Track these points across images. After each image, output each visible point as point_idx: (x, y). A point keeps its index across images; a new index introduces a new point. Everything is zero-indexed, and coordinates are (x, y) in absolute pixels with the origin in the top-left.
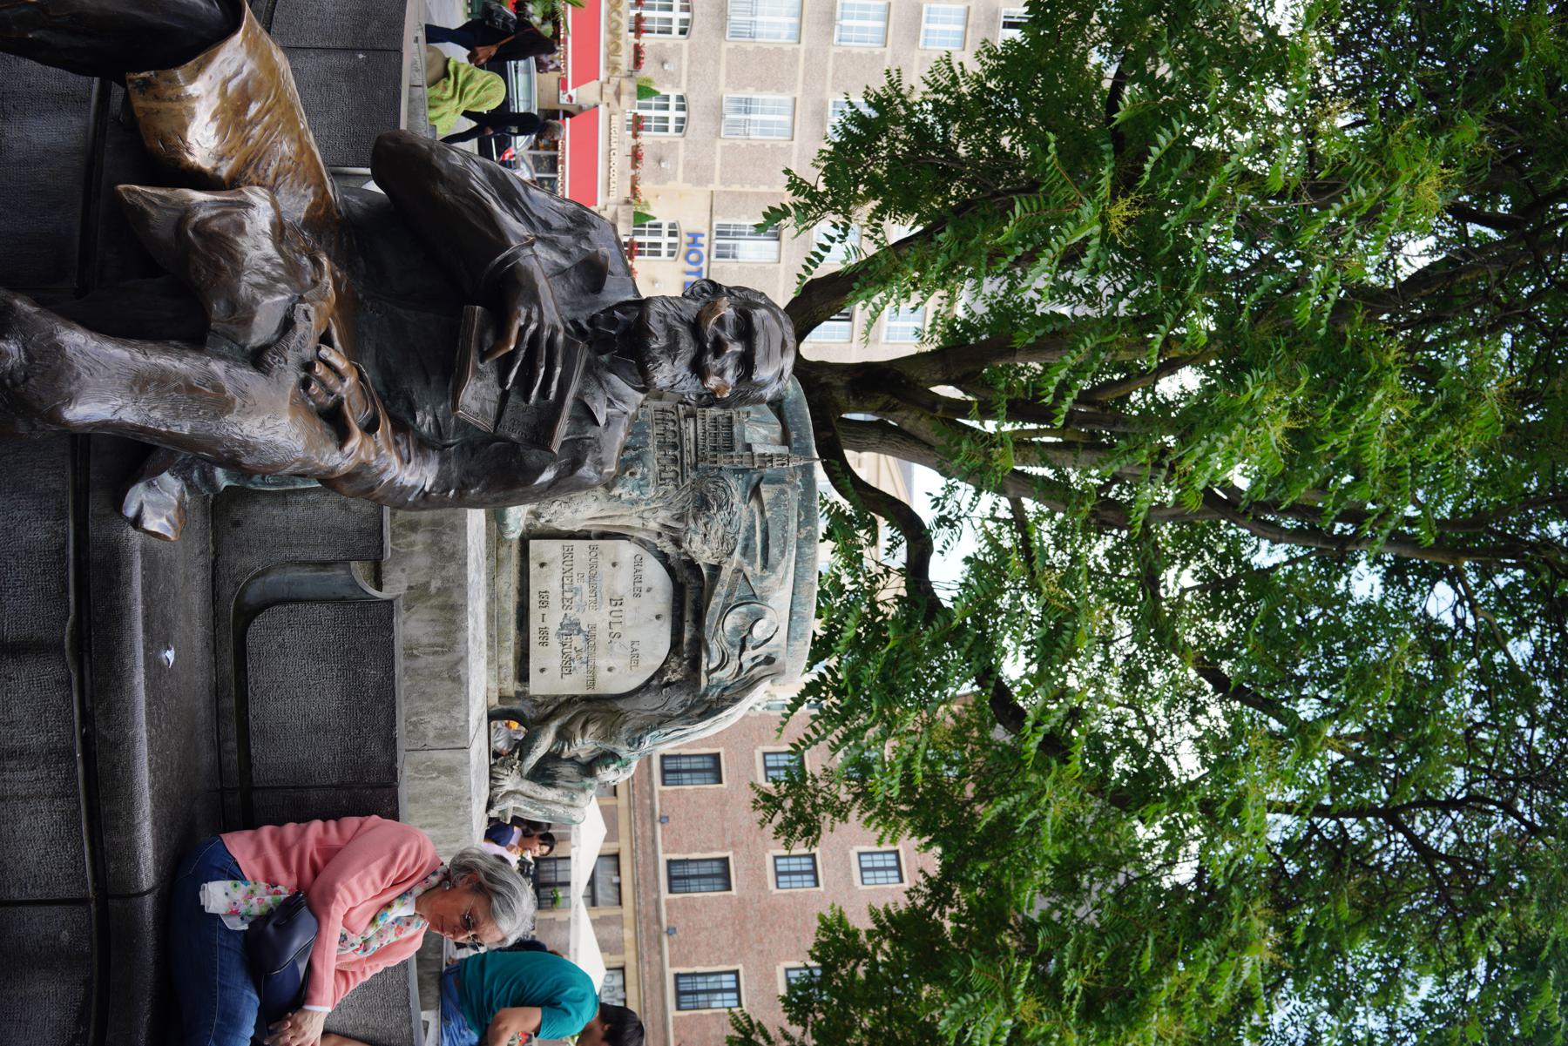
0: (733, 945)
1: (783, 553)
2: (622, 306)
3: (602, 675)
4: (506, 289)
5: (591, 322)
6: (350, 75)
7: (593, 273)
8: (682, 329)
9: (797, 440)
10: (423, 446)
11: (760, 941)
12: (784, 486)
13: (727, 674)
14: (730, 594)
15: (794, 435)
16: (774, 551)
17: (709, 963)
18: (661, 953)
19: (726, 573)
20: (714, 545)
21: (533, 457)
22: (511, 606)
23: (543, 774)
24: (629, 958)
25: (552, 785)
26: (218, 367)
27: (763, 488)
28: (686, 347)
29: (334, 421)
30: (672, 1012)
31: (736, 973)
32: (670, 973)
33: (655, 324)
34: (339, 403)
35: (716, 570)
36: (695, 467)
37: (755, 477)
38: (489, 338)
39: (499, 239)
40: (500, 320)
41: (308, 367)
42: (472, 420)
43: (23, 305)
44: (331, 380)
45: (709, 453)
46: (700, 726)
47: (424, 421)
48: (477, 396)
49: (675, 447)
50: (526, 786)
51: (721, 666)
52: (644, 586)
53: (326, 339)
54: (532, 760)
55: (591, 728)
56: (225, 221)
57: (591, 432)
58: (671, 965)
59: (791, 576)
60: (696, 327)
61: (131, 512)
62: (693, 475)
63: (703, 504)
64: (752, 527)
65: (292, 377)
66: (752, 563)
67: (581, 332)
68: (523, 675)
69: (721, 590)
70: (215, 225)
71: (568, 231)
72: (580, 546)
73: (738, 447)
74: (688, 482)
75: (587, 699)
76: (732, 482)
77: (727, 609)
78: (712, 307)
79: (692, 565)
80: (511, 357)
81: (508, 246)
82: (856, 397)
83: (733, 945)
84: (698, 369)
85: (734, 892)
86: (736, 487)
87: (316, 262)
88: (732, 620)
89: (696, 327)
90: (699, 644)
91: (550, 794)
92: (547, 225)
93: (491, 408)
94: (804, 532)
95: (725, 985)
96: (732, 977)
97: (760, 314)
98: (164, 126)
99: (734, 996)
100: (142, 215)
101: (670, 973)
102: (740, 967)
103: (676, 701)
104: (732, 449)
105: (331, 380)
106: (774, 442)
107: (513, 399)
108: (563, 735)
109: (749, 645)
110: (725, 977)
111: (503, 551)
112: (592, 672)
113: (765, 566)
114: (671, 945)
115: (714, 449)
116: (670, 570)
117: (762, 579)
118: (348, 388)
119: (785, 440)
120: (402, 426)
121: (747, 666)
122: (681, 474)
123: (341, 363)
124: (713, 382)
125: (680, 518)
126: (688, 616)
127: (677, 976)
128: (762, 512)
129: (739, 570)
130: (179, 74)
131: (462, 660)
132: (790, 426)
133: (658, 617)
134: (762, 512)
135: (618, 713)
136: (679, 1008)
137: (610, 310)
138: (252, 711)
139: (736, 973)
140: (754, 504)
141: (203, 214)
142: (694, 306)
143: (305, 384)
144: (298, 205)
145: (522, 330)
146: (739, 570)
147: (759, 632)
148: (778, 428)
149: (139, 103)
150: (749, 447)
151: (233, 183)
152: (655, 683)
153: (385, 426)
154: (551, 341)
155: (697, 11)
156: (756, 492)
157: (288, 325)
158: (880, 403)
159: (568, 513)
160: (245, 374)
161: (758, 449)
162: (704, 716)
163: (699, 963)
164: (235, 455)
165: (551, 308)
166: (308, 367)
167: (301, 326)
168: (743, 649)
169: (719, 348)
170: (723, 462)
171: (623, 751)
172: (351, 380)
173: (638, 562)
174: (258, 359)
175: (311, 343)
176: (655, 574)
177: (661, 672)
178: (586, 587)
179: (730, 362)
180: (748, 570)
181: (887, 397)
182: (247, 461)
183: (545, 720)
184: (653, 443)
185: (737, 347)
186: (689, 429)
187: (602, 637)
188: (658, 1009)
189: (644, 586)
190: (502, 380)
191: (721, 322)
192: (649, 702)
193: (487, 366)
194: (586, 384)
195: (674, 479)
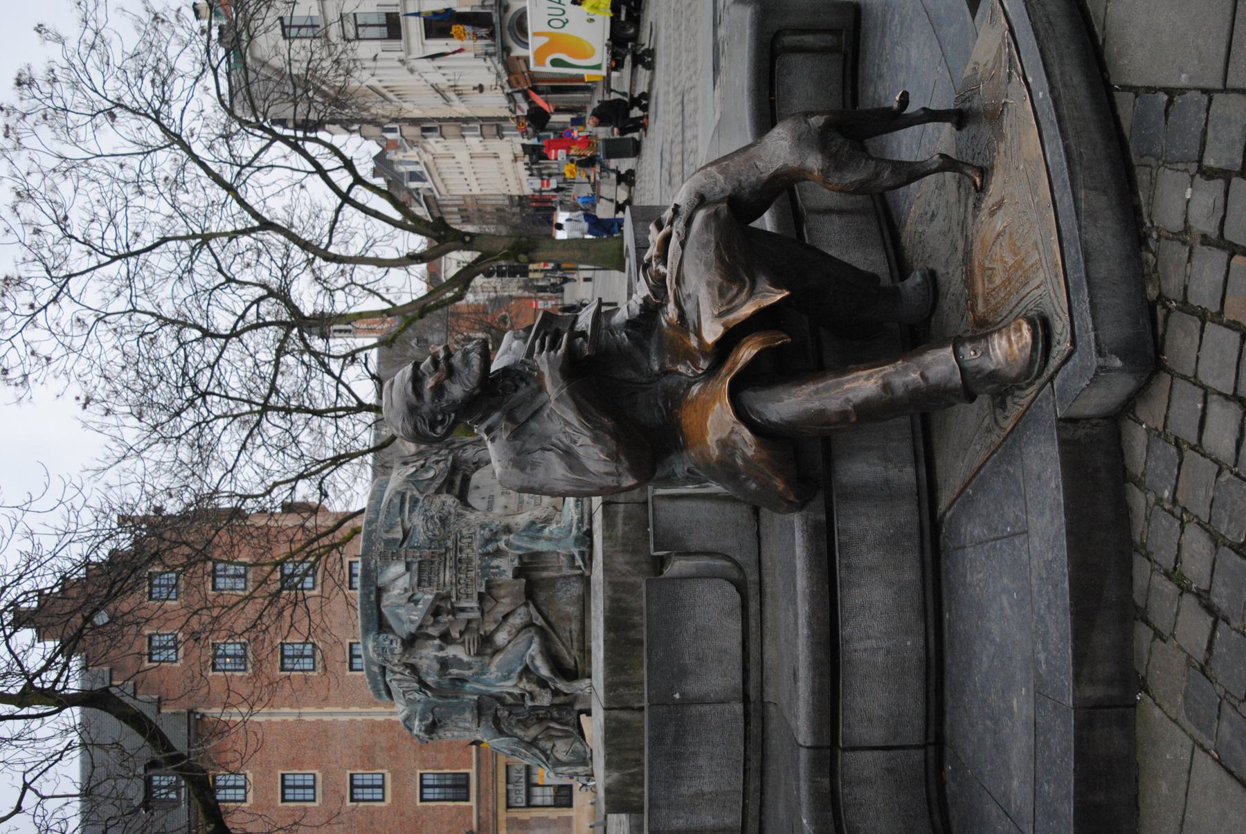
0: (423, 821)
1: (391, 500)
6: (683, 673)
9: (371, 592)
11: (401, 824)
12: (385, 536)
15: (373, 597)
16: (397, 501)
17: (442, 808)
18: (479, 817)
24: (503, 814)
27: (400, 536)
30: (472, 772)
31: (422, 800)
32: (473, 802)
36: (447, 549)
45: (437, 560)
49: (460, 561)
56: (729, 296)
58: (471, 807)
62: (450, 544)
64: (411, 512)
66: (412, 497)
73: (415, 567)
74: (453, 537)
83: (423, 821)
86: (420, 537)
94: (373, 526)
95: (431, 790)
96: (425, 797)
99: (425, 782)
101: (473, 802)
102: (419, 804)
110: (431, 797)
113: (403, 495)
114: (471, 823)
115: (432, 563)
125: (459, 515)
127: (467, 800)
128: (403, 521)
132: (374, 605)
133: (478, 487)
134: (403, 521)
136: (467, 775)
139: (422, 800)
140: (408, 525)
156: (406, 534)
163: (450, 809)
180: (416, 493)
184: (477, 562)
186: (448, 576)
188: (482, 775)
195: (462, 537)
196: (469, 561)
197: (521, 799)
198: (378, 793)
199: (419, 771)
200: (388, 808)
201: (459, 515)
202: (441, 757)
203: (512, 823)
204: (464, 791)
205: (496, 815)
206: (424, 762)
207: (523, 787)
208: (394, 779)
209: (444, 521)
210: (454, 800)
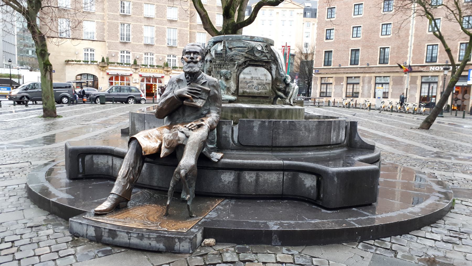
2: (185, 76)
3: (267, 82)
4: (181, 98)
5: (188, 82)
6: (149, 123)
7: (179, 81)
8: (189, 65)
10: (209, 112)
11: (373, 42)
13: (268, 55)
14: (251, 55)
17: (377, 55)
19: (246, 55)
20: (241, 58)
21: (211, 93)
22: (251, 99)
23: (286, 94)
25: (289, 92)
26: (188, 142)
28: (191, 64)
29: (199, 126)
30: (388, 65)
33: (188, 70)
34: (197, 125)
35: (246, 57)
37: (228, 49)
38: (189, 100)
39: (172, 97)
40: (186, 98)
41: (189, 129)
42: (203, 104)
43: (176, 170)
44: (192, 126)
46: (279, 61)
47: (205, 112)
48: (199, 103)
50: (289, 98)
51: (267, 57)
52: (249, 73)
53: (185, 127)
54: (284, 96)
55: (278, 84)
57: (207, 83)
59: (248, 42)
60: (189, 62)
61: (217, 161)
63: (232, 60)
65: (191, 132)
67: (189, 84)
68: (267, 97)
69: (250, 56)
70: (167, 143)
71: (172, 85)
72: (240, 85)
73: (222, 52)
75: (272, 85)
76: (228, 54)
77: (254, 55)
78: (185, 59)
79: (245, 62)
80: (192, 96)
81: (173, 96)
82: (230, 17)
84: (196, 62)
85: (360, 48)
87: (174, 128)
88: (257, 55)
89: (189, 62)
90: (261, 61)
91: (291, 93)
92: (172, 89)
93: (202, 100)
97: (187, 51)
98: (152, 150)
100: (166, 154)
103: (274, 67)
104: (222, 54)
105: (192, 126)
106: (221, 44)
107: (201, 97)
108: (280, 90)
109: (262, 50)
111: (240, 100)
112: (267, 83)
114: (371, 65)
116: (246, 67)
117: (248, 48)
118: (195, 124)
119: (220, 42)
120: (205, 116)
121: (267, 51)
122: (226, 64)
123: (190, 124)
124: (198, 59)
126: (256, 63)
127: (379, 63)
129: (246, 53)
130: (143, 147)
131: (257, 108)
135: (276, 79)
137: (186, 78)
138: (257, 145)
141: (166, 145)
142: (186, 64)
143: (192, 130)
144: (166, 130)
145: (188, 94)
146: (246, 53)
147: (260, 48)
148: (219, 44)
149: (148, 153)
150: (222, 50)
151: (162, 140)
152: (270, 70)
153: (204, 119)
154: (190, 89)
155: (148, 51)
157: (182, 132)
158: (232, 12)
159: (233, 88)
160: (190, 138)
161: (222, 48)
162: (277, 61)
163: (377, 58)
164: (203, 141)
165: (184, 89)
166: (189, 129)
167: (183, 130)
168: (263, 52)
169: (192, 58)
170: (224, 55)
171: (283, 78)
172: (193, 123)
173: (244, 74)
174: (188, 137)
175: (185, 128)
176: (247, 70)
177: (268, 69)
178: (249, 84)
179: (195, 56)
180: (246, 51)
181: (230, 10)
182: (204, 139)
183: (276, 93)
185: (192, 54)
187: (259, 81)
188: (387, 68)
189: (249, 73)
190: (197, 98)
191: (187, 58)
192: (274, 72)
193: (194, 100)
194: (198, 84)
196: (220, 68)
197: (378, 80)
198: (355, 36)
199: (390, 47)
200: (378, 37)
201: (235, 65)
202: (395, 54)
203: (370, 78)
204: (382, 62)
205: (374, 73)
206: (393, 49)
207: (383, 82)
208: (389, 38)
209: (232, 60)
210: (380, 59)
